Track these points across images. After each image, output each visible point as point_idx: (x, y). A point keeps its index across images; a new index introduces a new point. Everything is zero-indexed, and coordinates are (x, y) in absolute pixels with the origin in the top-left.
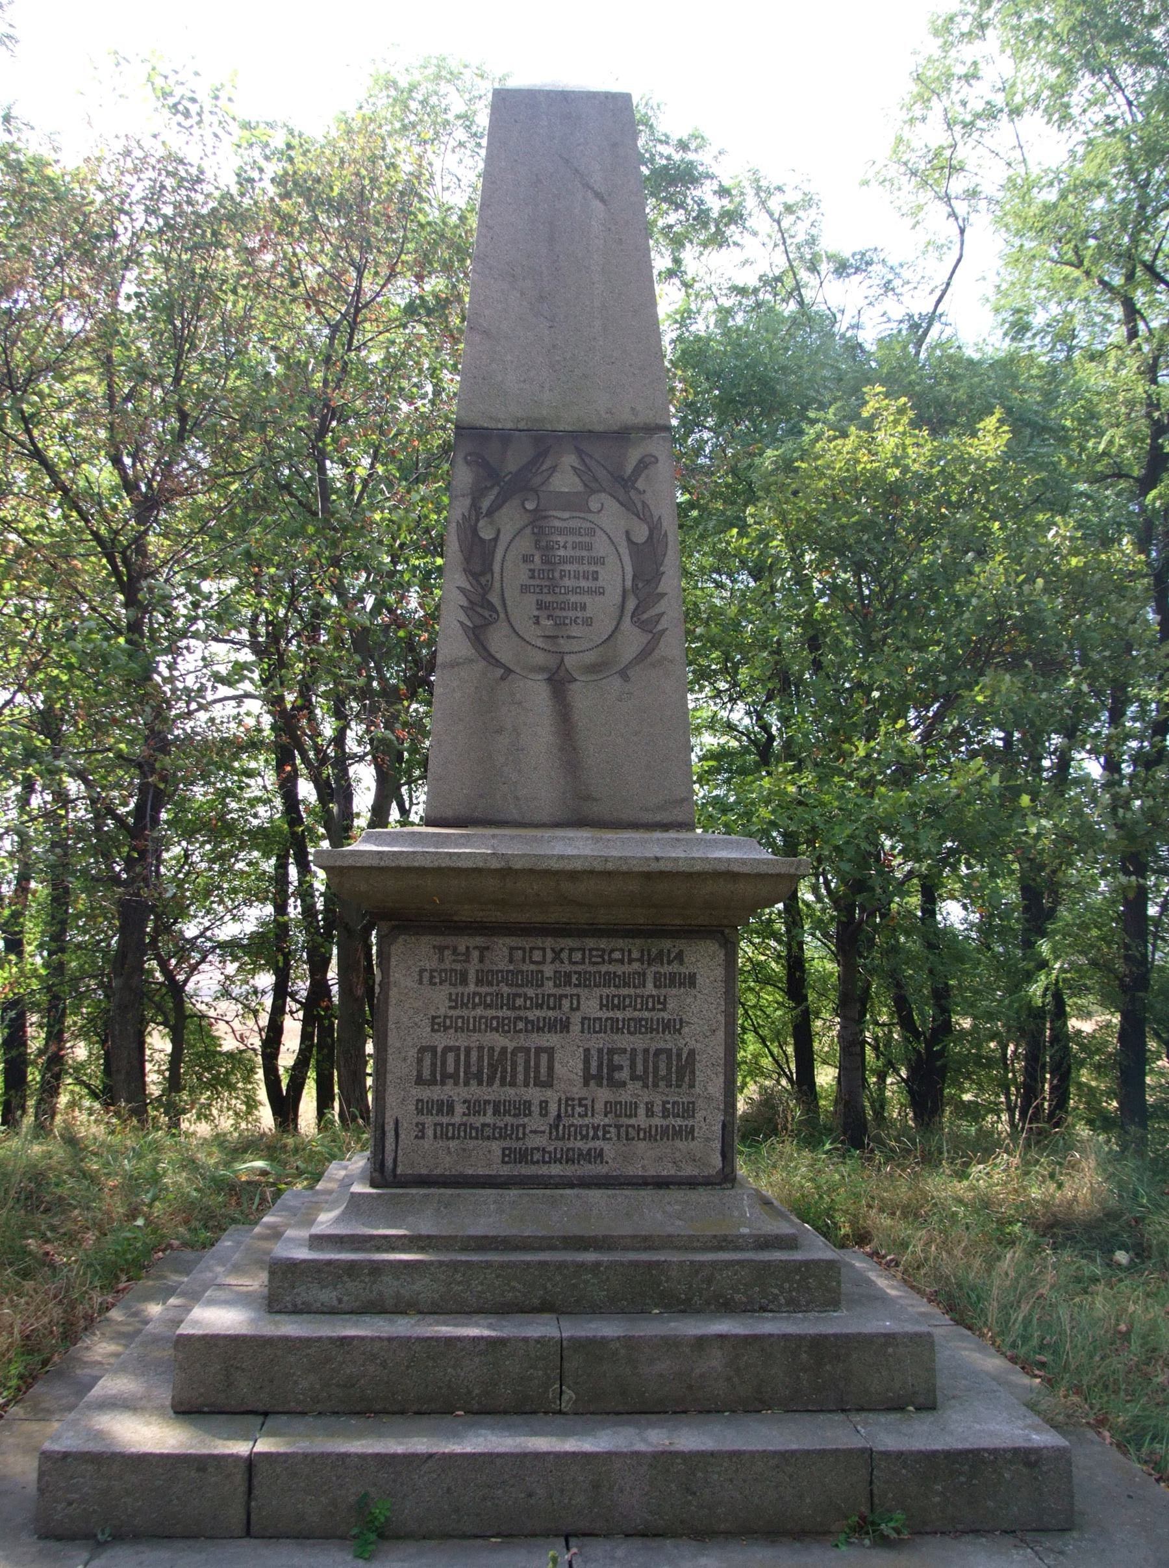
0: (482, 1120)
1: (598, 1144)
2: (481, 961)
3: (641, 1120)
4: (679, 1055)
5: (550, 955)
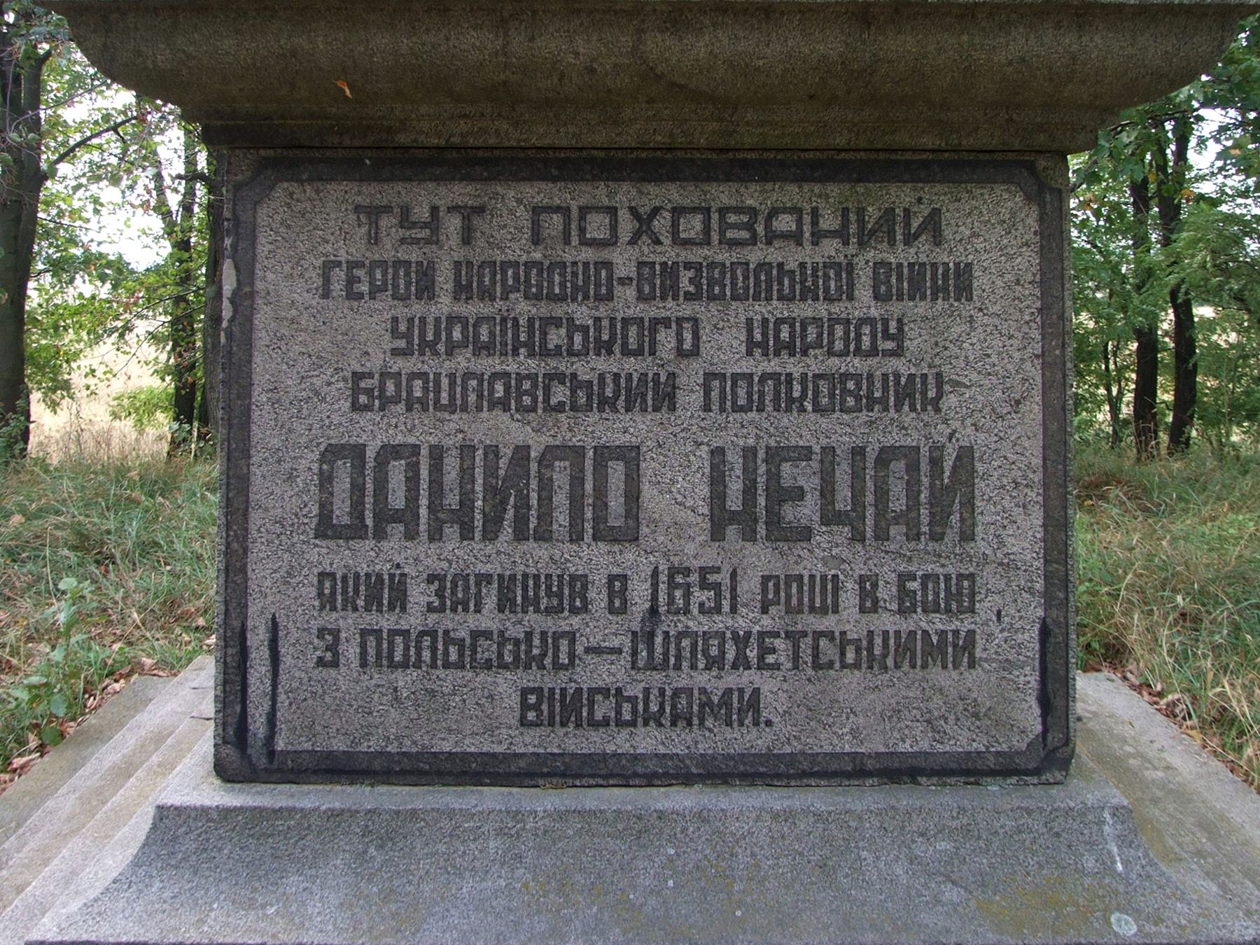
0: (473, 621)
1: (748, 678)
2: (467, 240)
3: (848, 619)
4: (936, 463)
5: (626, 225)
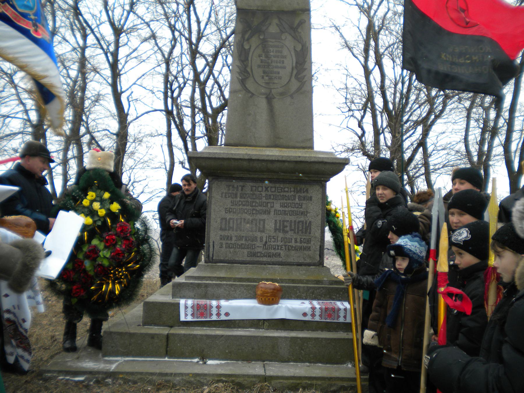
0: (241, 242)
1: (279, 251)
2: (242, 190)
3: (293, 244)
4: (306, 223)
5: (264, 189)
